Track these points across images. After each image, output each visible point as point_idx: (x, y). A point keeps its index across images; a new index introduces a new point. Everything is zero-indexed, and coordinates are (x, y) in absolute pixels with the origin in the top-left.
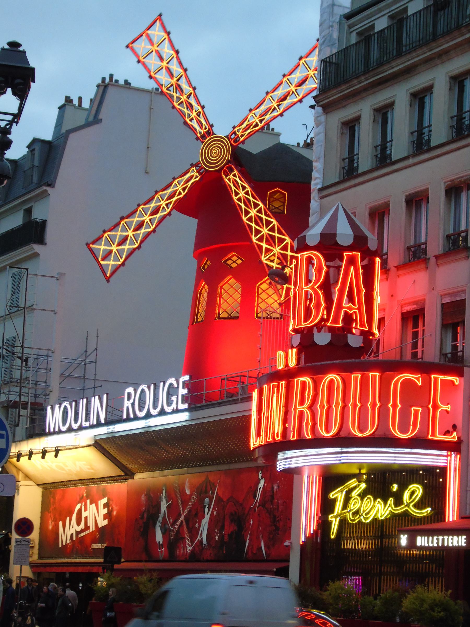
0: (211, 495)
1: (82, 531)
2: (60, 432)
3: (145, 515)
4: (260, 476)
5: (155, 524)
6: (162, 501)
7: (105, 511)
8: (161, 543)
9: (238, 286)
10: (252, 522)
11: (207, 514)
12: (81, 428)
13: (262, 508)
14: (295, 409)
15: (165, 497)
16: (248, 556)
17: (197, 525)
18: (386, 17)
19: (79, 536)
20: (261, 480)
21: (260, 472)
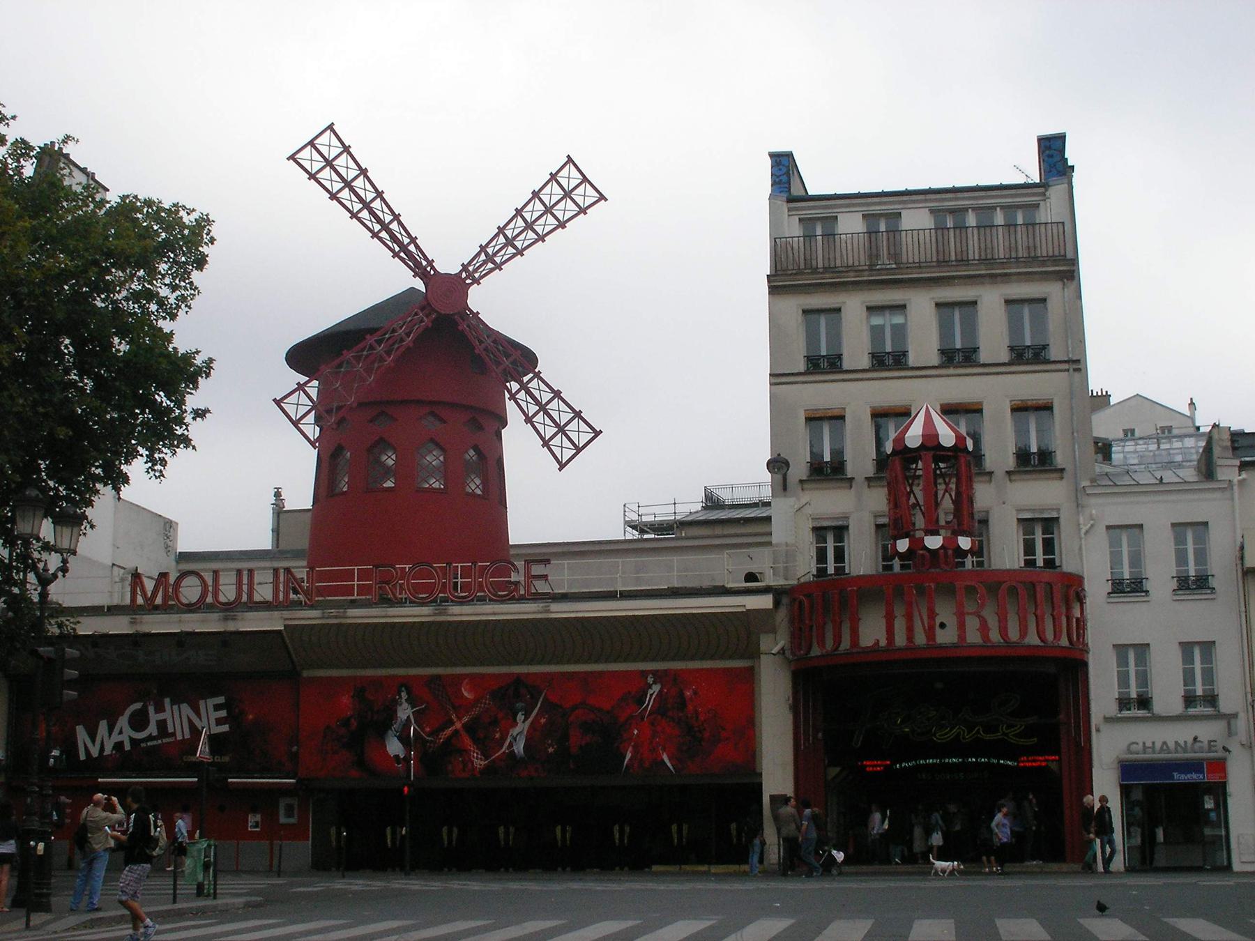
1: (150, 738)
3: (354, 724)
4: (650, 680)
6: (401, 705)
7: (223, 713)
11: (524, 722)
13: (659, 717)
17: (498, 736)
18: (861, 214)
19: (143, 745)
20: (653, 685)
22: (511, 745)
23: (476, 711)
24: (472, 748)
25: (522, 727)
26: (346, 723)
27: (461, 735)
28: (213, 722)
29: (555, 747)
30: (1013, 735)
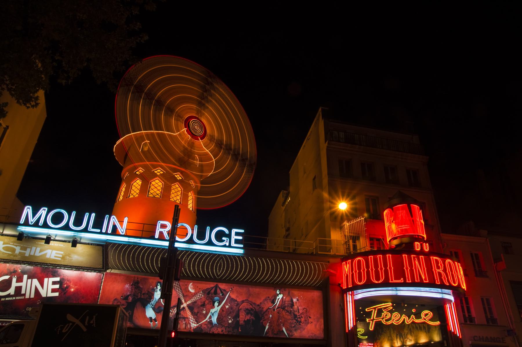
0: (222, 296)
2: (45, 225)
3: (130, 299)
4: (278, 292)
5: (144, 306)
7: (57, 286)
8: (153, 318)
9: (179, 189)
10: (271, 316)
11: (218, 306)
12: (86, 230)
13: (282, 310)
14: (436, 271)
15: (160, 290)
16: (268, 335)
17: (204, 312)
20: (279, 295)
21: (278, 290)
22: (210, 317)
23: (193, 300)
24: (191, 318)
25: (216, 309)
26: (126, 298)
27: (186, 310)
28: (50, 290)
29: (232, 320)
30: (360, 335)
